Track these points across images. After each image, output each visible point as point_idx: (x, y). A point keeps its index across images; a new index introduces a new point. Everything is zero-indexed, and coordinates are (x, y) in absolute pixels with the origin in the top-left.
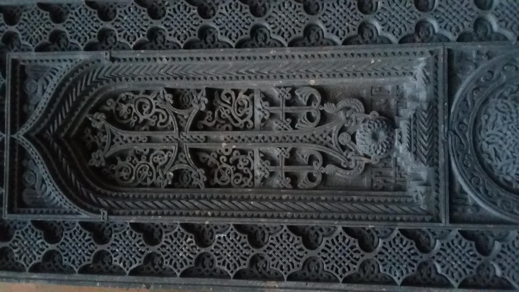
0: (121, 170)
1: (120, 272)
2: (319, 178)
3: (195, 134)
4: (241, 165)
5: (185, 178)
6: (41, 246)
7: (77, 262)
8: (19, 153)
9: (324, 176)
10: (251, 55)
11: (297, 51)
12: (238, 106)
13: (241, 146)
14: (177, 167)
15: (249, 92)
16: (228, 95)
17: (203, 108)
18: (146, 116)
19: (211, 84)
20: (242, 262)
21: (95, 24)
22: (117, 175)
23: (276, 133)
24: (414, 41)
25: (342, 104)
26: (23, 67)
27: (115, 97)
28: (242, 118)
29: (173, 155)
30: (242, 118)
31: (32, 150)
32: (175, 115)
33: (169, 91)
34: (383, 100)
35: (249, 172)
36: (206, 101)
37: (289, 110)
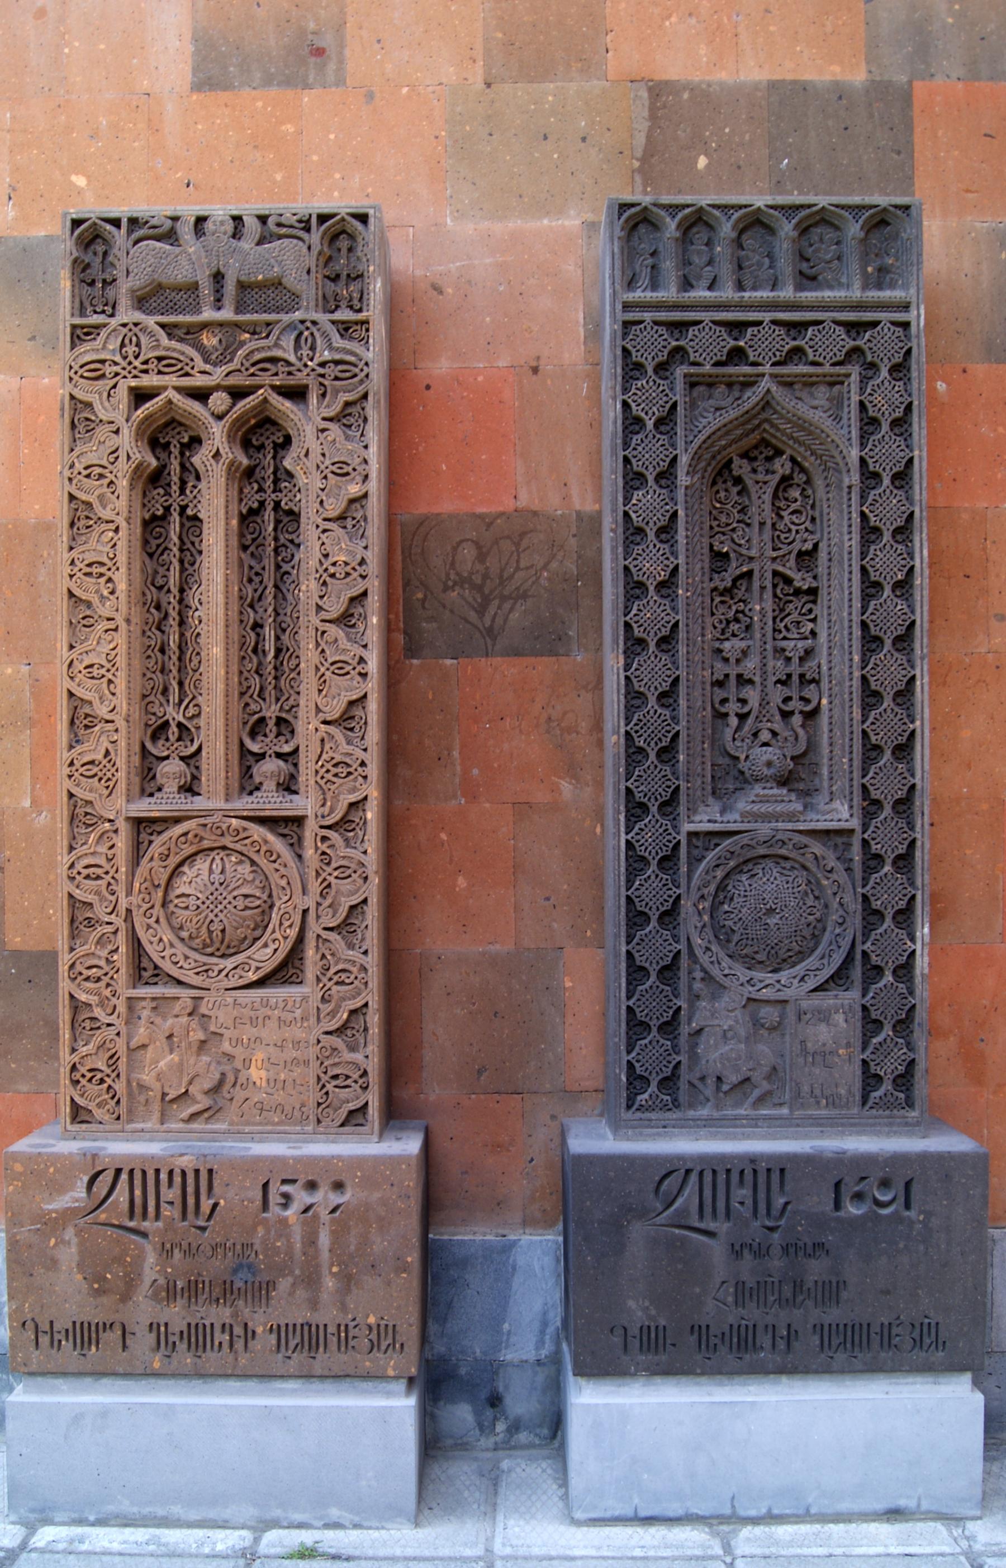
0: (726, 490)
1: (627, 500)
2: (723, 710)
3: (769, 575)
4: (734, 627)
5: (719, 564)
6: (650, 412)
7: (635, 453)
8: (748, 384)
9: (727, 715)
10: (854, 636)
11: (856, 683)
12: (798, 623)
13: (757, 626)
14: (732, 555)
15: (813, 633)
16: (810, 611)
17: (797, 584)
18: (787, 519)
19: (823, 593)
20: (642, 629)
21: (888, 468)
22: (720, 486)
23: (771, 663)
24: (864, 800)
25: (801, 732)
26: (842, 383)
27: (808, 482)
28: (786, 627)
29: (744, 552)
30: (786, 627)
31: (752, 397)
32: (790, 553)
33: (816, 546)
34: (803, 776)
35: (727, 635)
36: (805, 587)
37: (795, 678)
